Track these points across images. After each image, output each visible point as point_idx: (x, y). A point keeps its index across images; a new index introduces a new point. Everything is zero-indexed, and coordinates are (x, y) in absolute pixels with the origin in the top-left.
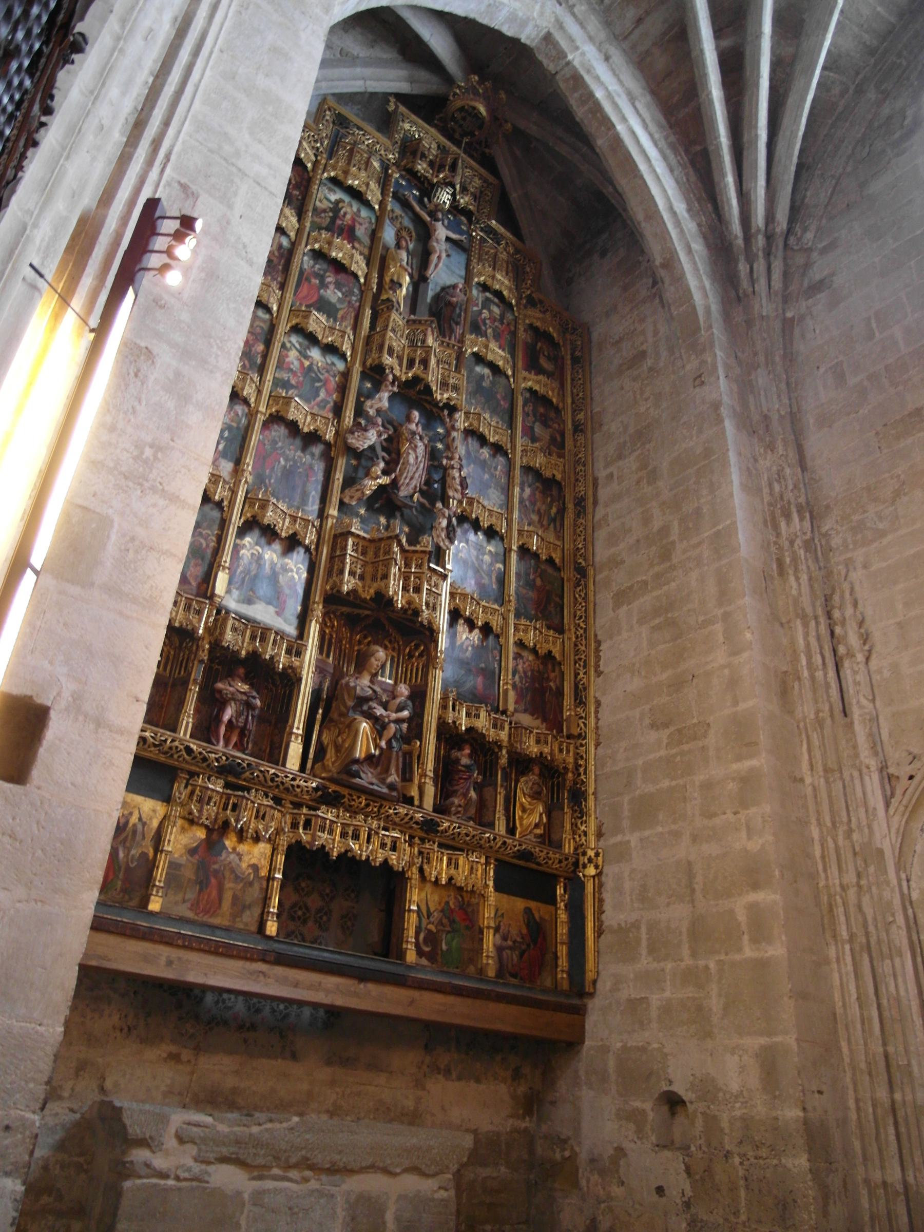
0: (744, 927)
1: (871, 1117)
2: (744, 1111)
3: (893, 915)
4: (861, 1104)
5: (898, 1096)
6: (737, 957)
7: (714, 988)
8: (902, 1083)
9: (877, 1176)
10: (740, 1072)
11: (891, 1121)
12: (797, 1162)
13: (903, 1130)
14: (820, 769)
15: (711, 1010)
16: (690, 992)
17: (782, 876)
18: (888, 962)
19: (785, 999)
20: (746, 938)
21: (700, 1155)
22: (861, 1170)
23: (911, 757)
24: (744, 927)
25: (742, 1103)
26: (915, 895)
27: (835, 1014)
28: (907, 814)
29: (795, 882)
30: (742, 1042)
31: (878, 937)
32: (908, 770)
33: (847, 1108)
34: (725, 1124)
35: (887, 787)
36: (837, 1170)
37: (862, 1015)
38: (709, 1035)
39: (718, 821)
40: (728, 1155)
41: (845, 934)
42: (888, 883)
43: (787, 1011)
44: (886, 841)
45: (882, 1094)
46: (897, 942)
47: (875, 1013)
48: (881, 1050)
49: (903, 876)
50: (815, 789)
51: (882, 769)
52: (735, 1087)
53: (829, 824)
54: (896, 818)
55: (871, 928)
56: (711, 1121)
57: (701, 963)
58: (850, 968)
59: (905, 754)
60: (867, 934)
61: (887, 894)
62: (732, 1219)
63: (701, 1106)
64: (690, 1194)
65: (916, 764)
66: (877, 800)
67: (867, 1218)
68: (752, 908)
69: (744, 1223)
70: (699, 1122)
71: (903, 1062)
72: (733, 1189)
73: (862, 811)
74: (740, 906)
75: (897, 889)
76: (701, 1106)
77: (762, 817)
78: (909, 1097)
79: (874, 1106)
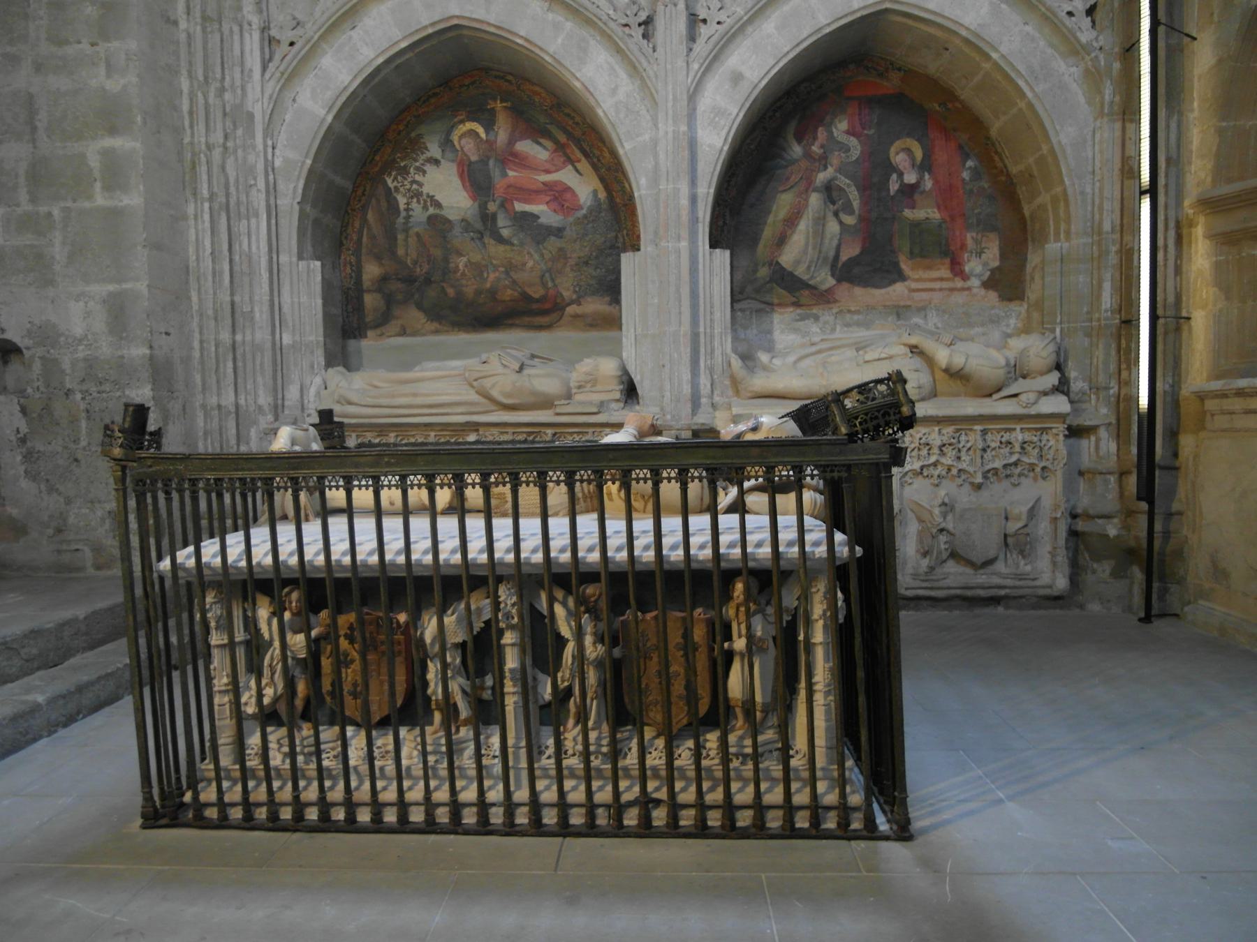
0: (97, 174)
1: (213, 355)
2: (89, 353)
3: (255, 179)
4: (205, 345)
5: (239, 337)
6: (87, 205)
7: (57, 237)
8: (244, 326)
9: (214, 400)
10: (85, 318)
11: (230, 357)
12: (140, 392)
13: (240, 364)
14: (198, 14)
15: (53, 257)
16: (28, 239)
17: (145, 123)
18: (244, 222)
19: (139, 248)
20: (98, 185)
21: (38, 395)
22: (200, 397)
23: (294, 23)
24: (97, 174)
25: (86, 346)
26: (278, 163)
27: (187, 267)
28: (282, 81)
29: (159, 132)
30: (87, 289)
31: (238, 198)
32: (288, 35)
33: (192, 348)
34: (66, 365)
35: (267, 50)
37: (214, 268)
38: (51, 282)
39: (70, 50)
40: (68, 393)
41: (205, 193)
42: (254, 147)
43: (140, 259)
44: (258, 108)
45: (225, 336)
46: (255, 204)
47: (226, 267)
48: (228, 299)
49: (270, 143)
50: (189, 36)
51: (264, 29)
52: (78, 331)
53: (201, 78)
54: (272, 83)
55: (232, 190)
56: (51, 366)
57: (43, 209)
58: (207, 224)
59: (289, 18)
60: (228, 195)
61: (251, 158)
62: (72, 446)
63: (40, 351)
64: (27, 430)
65: (299, 31)
66: (254, 61)
67: (201, 434)
68: (107, 154)
69: (84, 449)
70: (37, 367)
71: (246, 309)
72: (74, 421)
73: (237, 70)
74: (93, 150)
75: (262, 154)
76: (40, 351)
77: (127, 54)
78: (248, 338)
79: (217, 346)
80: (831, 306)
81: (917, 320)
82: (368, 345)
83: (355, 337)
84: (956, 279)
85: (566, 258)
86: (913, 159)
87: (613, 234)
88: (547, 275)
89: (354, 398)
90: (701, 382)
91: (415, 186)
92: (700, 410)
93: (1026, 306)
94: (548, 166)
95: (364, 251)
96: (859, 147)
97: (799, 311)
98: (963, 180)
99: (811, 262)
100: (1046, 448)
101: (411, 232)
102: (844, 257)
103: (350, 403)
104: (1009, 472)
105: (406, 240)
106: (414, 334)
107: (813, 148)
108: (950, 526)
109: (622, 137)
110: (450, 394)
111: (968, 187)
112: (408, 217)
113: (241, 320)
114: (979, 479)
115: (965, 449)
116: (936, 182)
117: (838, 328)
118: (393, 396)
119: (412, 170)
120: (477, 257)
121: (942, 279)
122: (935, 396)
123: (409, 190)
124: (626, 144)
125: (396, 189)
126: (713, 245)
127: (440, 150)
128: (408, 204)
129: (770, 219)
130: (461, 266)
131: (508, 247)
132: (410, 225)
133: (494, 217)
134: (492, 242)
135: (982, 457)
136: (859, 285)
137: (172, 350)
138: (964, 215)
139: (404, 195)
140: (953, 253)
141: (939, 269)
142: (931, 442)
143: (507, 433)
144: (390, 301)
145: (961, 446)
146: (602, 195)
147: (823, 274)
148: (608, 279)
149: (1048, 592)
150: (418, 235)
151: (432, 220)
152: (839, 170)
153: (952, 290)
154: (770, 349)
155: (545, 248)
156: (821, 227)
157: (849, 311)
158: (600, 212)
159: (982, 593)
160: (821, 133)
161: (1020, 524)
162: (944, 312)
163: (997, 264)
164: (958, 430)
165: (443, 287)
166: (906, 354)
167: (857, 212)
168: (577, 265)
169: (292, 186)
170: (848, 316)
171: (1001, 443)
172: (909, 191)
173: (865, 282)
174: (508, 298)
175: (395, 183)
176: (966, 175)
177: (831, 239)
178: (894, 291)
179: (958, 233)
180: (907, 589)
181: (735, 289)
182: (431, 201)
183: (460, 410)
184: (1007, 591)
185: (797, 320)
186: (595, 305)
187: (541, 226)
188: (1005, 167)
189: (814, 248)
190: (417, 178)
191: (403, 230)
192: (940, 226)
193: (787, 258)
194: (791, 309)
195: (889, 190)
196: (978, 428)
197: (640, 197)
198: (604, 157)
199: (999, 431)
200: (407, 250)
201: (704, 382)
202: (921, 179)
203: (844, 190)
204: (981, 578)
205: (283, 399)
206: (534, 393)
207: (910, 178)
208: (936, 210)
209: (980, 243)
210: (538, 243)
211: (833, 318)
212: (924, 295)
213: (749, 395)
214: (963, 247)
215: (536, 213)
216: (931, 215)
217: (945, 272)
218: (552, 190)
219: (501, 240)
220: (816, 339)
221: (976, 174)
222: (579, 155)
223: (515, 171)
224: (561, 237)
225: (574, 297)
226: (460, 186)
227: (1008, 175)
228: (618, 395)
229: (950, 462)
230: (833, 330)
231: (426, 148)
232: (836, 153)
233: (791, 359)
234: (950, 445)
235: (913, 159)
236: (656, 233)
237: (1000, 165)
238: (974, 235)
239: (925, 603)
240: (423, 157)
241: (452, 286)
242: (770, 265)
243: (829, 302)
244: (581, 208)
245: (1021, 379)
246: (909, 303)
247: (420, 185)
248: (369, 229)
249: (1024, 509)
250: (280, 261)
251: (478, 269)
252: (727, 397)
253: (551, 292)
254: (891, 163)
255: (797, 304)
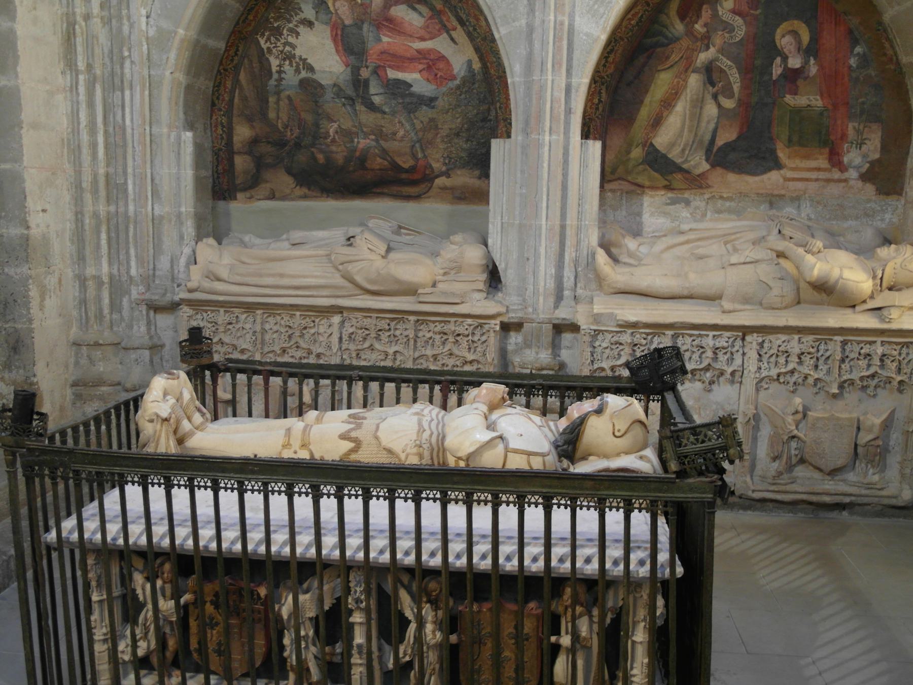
8: (117, 198)
12: (19, 271)
18: (119, 93)
29: (35, 9)
36: (54, 272)
71: (120, 181)
78: (122, 209)
80: (702, 191)
81: (790, 210)
82: (238, 208)
83: (225, 199)
84: (834, 169)
85: (436, 127)
86: (799, 42)
87: (486, 107)
88: (417, 145)
89: (224, 274)
90: (565, 275)
91: (288, 48)
92: (563, 303)
93: (903, 202)
94: (422, 33)
95: (235, 112)
96: (744, 28)
97: (670, 195)
98: (850, 67)
99: (686, 145)
100: (906, 361)
101: (283, 95)
102: (720, 142)
103: (219, 279)
104: (865, 383)
105: (277, 103)
106: (284, 198)
107: (697, 26)
108: (801, 435)
109: (498, 21)
110: (316, 277)
111: (854, 75)
112: (281, 79)
113: (115, 191)
114: (836, 391)
115: (824, 358)
116: (821, 67)
117: (709, 214)
118: (261, 276)
119: (285, 32)
120: (347, 124)
121: (819, 169)
122: (799, 303)
123: (282, 52)
124: (501, 29)
125: (269, 50)
126: (586, 134)
127: (314, 12)
128: (280, 66)
129: (647, 100)
130: (331, 131)
131: (379, 115)
132: (282, 88)
133: (366, 83)
134: (363, 108)
135: (840, 367)
136: (733, 171)
137: (48, 226)
138: (848, 103)
139: (277, 57)
140: (833, 142)
141: (817, 159)
142: (790, 350)
143: (370, 317)
144: (260, 165)
145: (820, 354)
146: (477, 66)
147: (698, 158)
148: (478, 153)
149: (894, 502)
150: (289, 97)
151: (305, 84)
152: (721, 51)
153: (828, 181)
154: (637, 233)
155: (416, 118)
156: (698, 110)
157: (721, 197)
158: (474, 84)
159: (827, 499)
160: (706, 13)
161: (870, 437)
162: (818, 203)
163: (877, 156)
164: (818, 340)
165: (313, 153)
166: (771, 259)
167: (736, 95)
168: (447, 136)
169: (164, 57)
170: (720, 202)
171: (860, 354)
172: (793, 77)
173: (739, 168)
174: (378, 167)
175: (268, 44)
176: (853, 62)
177: (708, 122)
178: (769, 179)
179: (839, 122)
180: (753, 491)
181: (607, 169)
182: (304, 65)
183: (325, 293)
184: (853, 498)
185: (667, 204)
186: (463, 178)
187: (412, 95)
188: (896, 54)
189: (690, 131)
190: (290, 39)
191: (275, 93)
192: (821, 114)
193: (661, 140)
194: (663, 193)
195: (772, 74)
196: (839, 338)
197: (513, 83)
198: (480, 27)
199: (859, 343)
200: (278, 114)
201: (568, 274)
202: (806, 62)
203: (725, 71)
204: (829, 485)
205: (154, 269)
206: (397, 281)
207: (795, 62)
208: (818, 97)
209: (862, 134)
210: (410, 113)
211: (704, 203)
212: (800, 185)
213: (612, 290)
214: (844, 137)
215: (409, 81)
216: (814, 103)
217: (823, 162)
218: (426, 59)
219: (372, 107)
220: (685, 227)
221: (864, 61)
222: (455, 23)
223: (390, 37)
224: (433, 107)
225: (444, 169)
226: (334, 50)
227: (898, 63)
228: (481, 286)
229: (806, 371)
230: (704, 215)
231: (300, 9)
232: (720, 33)
233: (660, 245)
234: (809, 353)
235: (799, 42)
236: (527, 123)
237: (890, 52)
238: (856, 124)
239: (771, 505)
240: (297, 18)
241: (321, 151)
242: (644, 145)
243: (701, 187)
244: (454, 78)
245: (887, 291)
246: (783, 192)
247: (293, 47)
248: (241, 89)
249: (878, 421)
250: (153, 132)
251: (348, 135)
252: (590, 290)
253: (421, 163)
254: (775, 46)
255: (668, 188)
